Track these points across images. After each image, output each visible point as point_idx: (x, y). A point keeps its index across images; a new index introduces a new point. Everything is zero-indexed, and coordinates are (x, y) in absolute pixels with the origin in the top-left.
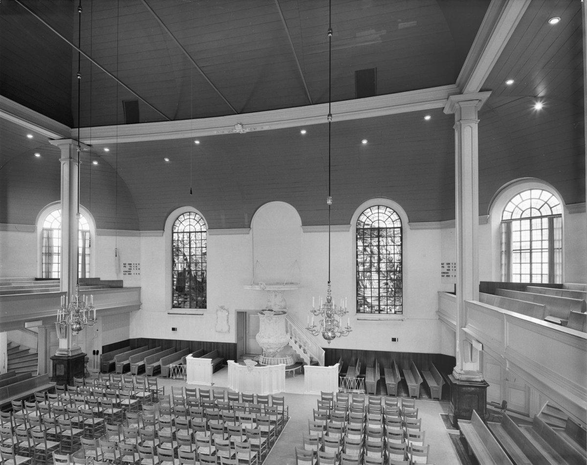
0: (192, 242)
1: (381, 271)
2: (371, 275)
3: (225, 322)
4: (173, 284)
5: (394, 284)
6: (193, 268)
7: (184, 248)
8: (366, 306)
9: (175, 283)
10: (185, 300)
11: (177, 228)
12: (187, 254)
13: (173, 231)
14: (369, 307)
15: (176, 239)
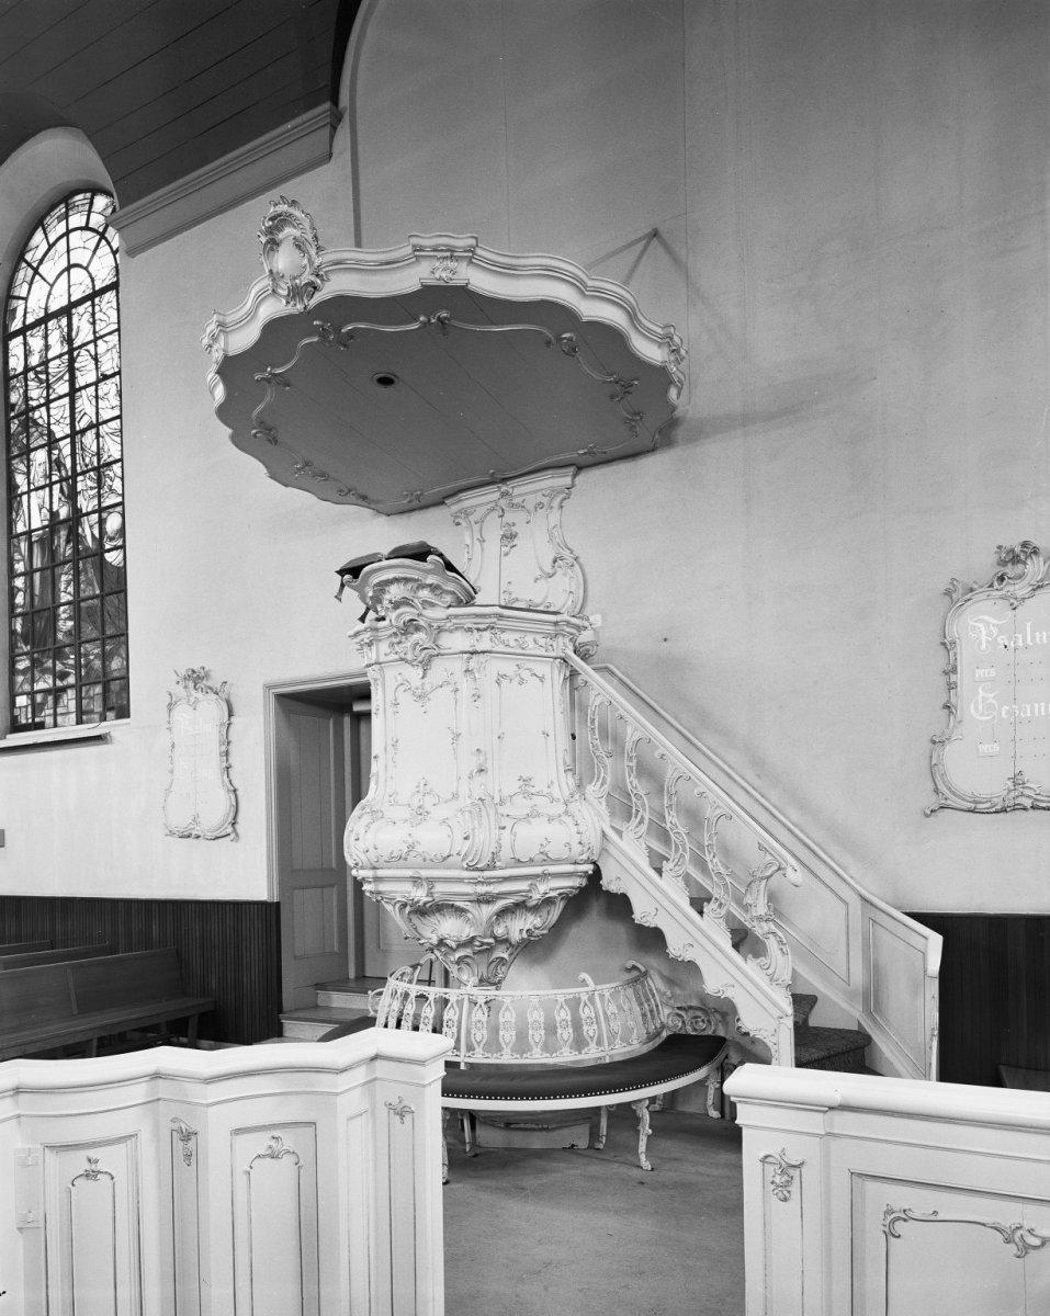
0: (83, 360)
3: (211, 770)
4: (12, 606)
6: (86, 503)
9: (19, 599)
10: (59, 683)
12: (61, 430)
15: (20, 369)
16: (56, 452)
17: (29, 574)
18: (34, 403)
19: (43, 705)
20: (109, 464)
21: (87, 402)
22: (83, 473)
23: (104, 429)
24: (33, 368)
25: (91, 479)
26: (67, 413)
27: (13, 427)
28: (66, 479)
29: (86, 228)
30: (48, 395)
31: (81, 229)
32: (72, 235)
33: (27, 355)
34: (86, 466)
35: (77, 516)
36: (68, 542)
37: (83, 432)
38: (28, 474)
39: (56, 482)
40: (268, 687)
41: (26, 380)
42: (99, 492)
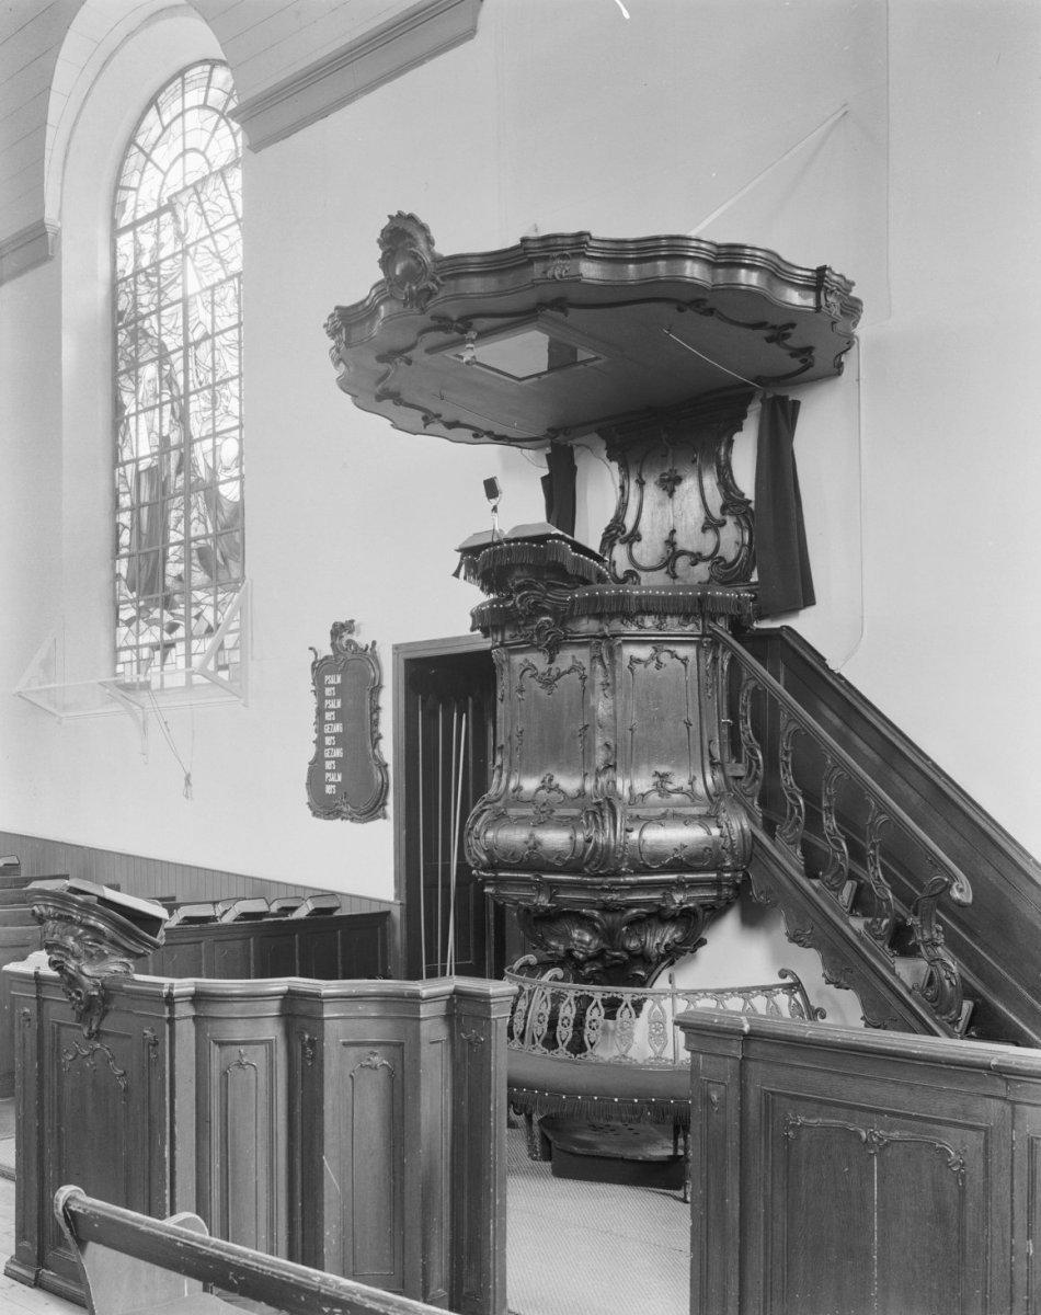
4: (117, 547)
6: (197, 429)
9: (125, 538)
10: (167, 637)
11: (130, 198)
12: (172, 342)
13: (114, 222)
15: (129, 272)
16: (167, 367)
17: (135, 509)
18: (144, 311)
19: (150, 659)
20: (225, 382)
21: (201, 309)
22: (196, 392)
23: (219, 340)
24: (144, 271)
25: (205, 398)
26: (180, 322)
27: (121, 338)
28: (181, 397)
29: (204, 106)
30: (160, 301)
31: (198, 107)
32: (188, 116)
33: (138, 253)
34: (201, 383)
35: (188, 441)
36: (178, 472)
38: (136, 392)
39: (166, 403)
40: (396, 647)
41: (135, 283)
42: (213, 414)
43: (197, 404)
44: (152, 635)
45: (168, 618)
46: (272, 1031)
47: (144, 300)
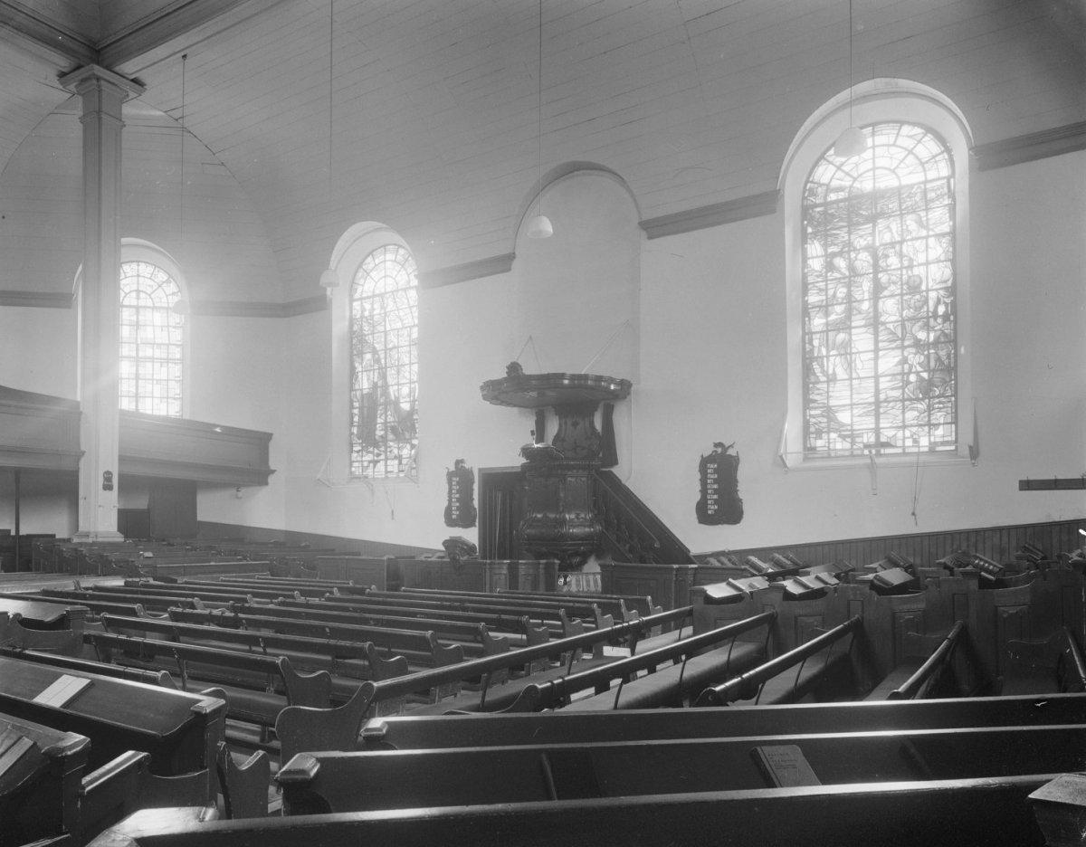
1: (884, 324)
2: (850, 340)
5: (928, 357)
6: (390, 380)
7: (373, 333)
8: (833, 435)
9: (356, 419)
14: (844, 437)
16: (377, 356)
17: (361, 408)
27: (354, 341)
31: (392, 261)
35: (386, 386)
36: (382, 396)
37: (391, 349)
43: (391, 373)
44: (369, 457)
45: (376, 451)
46: (505, 571)
47: (366, 328)
